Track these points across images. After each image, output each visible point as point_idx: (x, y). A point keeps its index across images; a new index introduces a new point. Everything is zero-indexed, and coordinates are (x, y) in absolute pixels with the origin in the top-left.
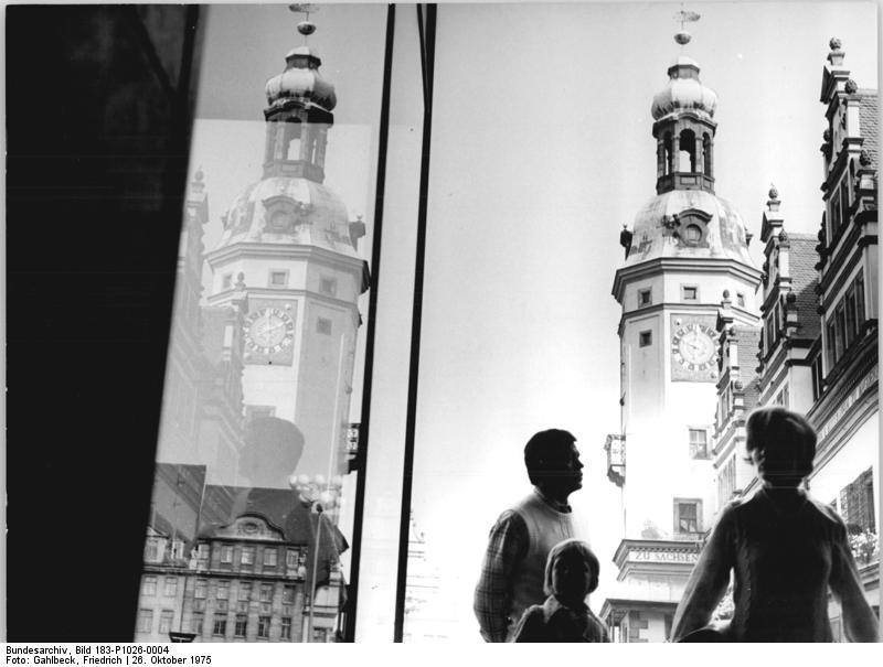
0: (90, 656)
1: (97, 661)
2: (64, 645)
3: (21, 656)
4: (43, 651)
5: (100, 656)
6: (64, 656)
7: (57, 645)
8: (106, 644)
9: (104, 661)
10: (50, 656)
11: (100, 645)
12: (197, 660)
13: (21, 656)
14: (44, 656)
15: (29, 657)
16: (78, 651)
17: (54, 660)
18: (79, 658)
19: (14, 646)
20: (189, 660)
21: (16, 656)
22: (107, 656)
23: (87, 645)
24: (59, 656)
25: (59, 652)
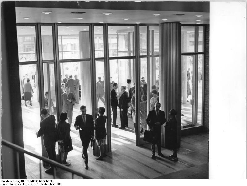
0: (25, 183)
2: (18, 180)
3: (6, 183)
4: (12, 182)
5: (28, 183)
7: (16, 180)
9: (29, 184)
12: (58, 184)
14: (12, 183)
16: (22, 181)
17: (15, 184)
18: (22, 183)
19: (4, 180)
21: (4, 183)
22: (30, 183)
24: (16, 183)
25: (17, 182)
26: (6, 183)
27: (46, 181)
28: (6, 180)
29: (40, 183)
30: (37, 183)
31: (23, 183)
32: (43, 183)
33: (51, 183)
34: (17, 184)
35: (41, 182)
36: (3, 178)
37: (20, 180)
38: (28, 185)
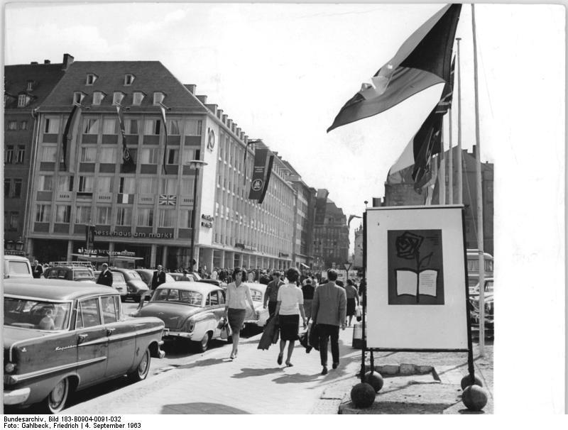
0: (58, 423)
1: (62, 426)
2: (41, 416)
3: (14, 423)
4: (28, 420)
5: (64, 423)
6: (41, 423)
7: (37, 416)
9: (67, 426)
10: (32, 423)
12: (134, 425)
14: (28, 423)
15: (19, 424)
16: (50, 419)
17: (35, 426)
18: (51, 424)
19: (9, 416)
20: (126, 426)
21: (10, 423)
22: (69, 423)
24: (38, 423)
25: (38, 420)
26: (14, 423)
27: (105, 419)
28: (15, 416)
30: (85, 423)
31: (52, 423)
32: (98, 423)
33: (119, 423)
34: (40, 426)
35: (93, 422)
36: (6, 412)
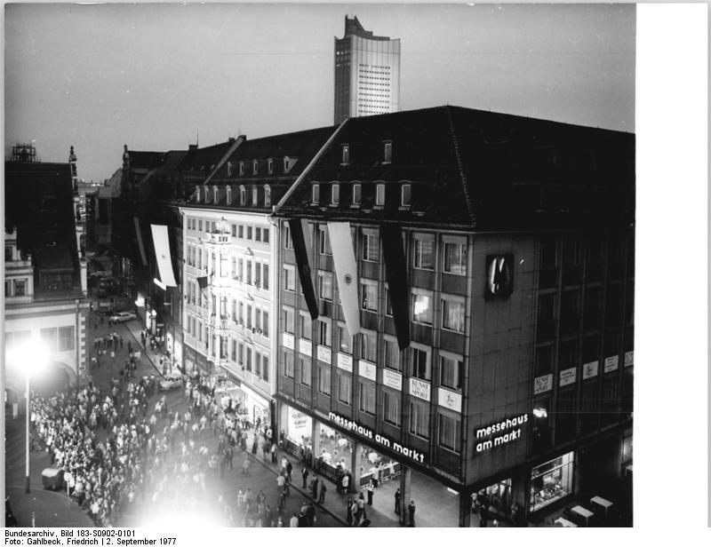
0: (73, 538)
1: (78, 542)
2: (51, 530)
3: (17, 538)
4: (35, 534)
5: (81, 538)
7: (46, 529)
8: (85, 529)
9: (84, 542)
10: (40, 538)
11: (80, 529)
13: (17, 538)
15: (25, 539)
16: (63, 534)
17: (43, 542)
18: (64, 540)
19: (12, 530)
21: (13, 538)
22: (86, 538)
23: (70, 529)
24: (47, 538)
25: (48, 535)
27: (123, 533)
28: (18, 530)
29: (114, 540)
34: (50, 542)
36: (8, 525)
37: (57, 531)
38: (81, 545)
